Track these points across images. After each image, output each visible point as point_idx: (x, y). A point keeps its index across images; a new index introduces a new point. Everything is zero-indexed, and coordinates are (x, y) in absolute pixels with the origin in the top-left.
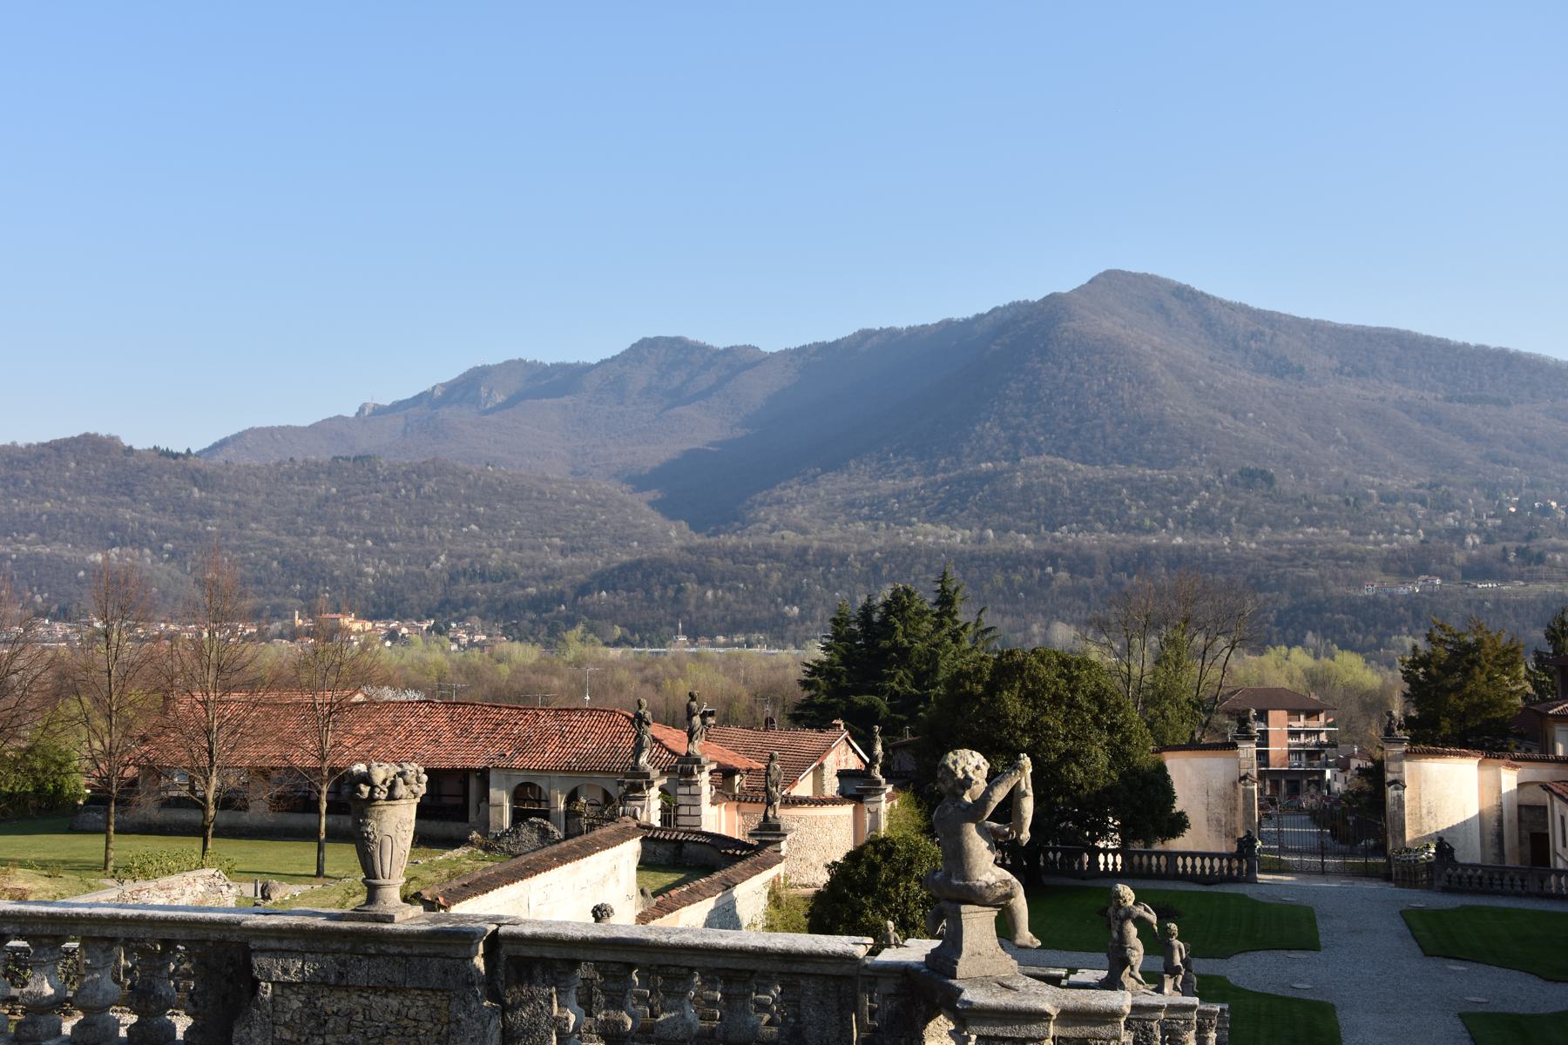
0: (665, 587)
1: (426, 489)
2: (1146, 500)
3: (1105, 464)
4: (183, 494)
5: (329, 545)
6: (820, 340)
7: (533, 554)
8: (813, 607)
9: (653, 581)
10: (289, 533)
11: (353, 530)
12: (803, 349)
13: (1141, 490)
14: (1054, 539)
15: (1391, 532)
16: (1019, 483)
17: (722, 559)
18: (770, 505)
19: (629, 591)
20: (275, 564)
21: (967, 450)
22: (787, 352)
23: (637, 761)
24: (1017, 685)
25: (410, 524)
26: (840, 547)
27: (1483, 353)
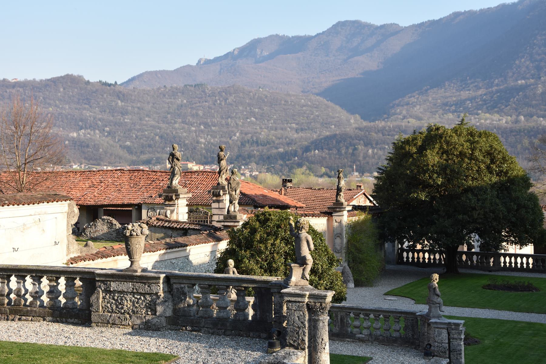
0: (347, 148)
1: (230, 100)
4: (113, 104)
5: (183, 128)
7: (282, 132)
9: (341, 145)
10: (164, 122)
11: (194, 121)
12: (422, 24)
17: (376, 133)
18: (402, 106)
19: (329, 149)
20: (157, 137)
21: (510, 74)
22: (414, 26)
23: (171, 182)
24: (437, 146)
25: (222, 118)
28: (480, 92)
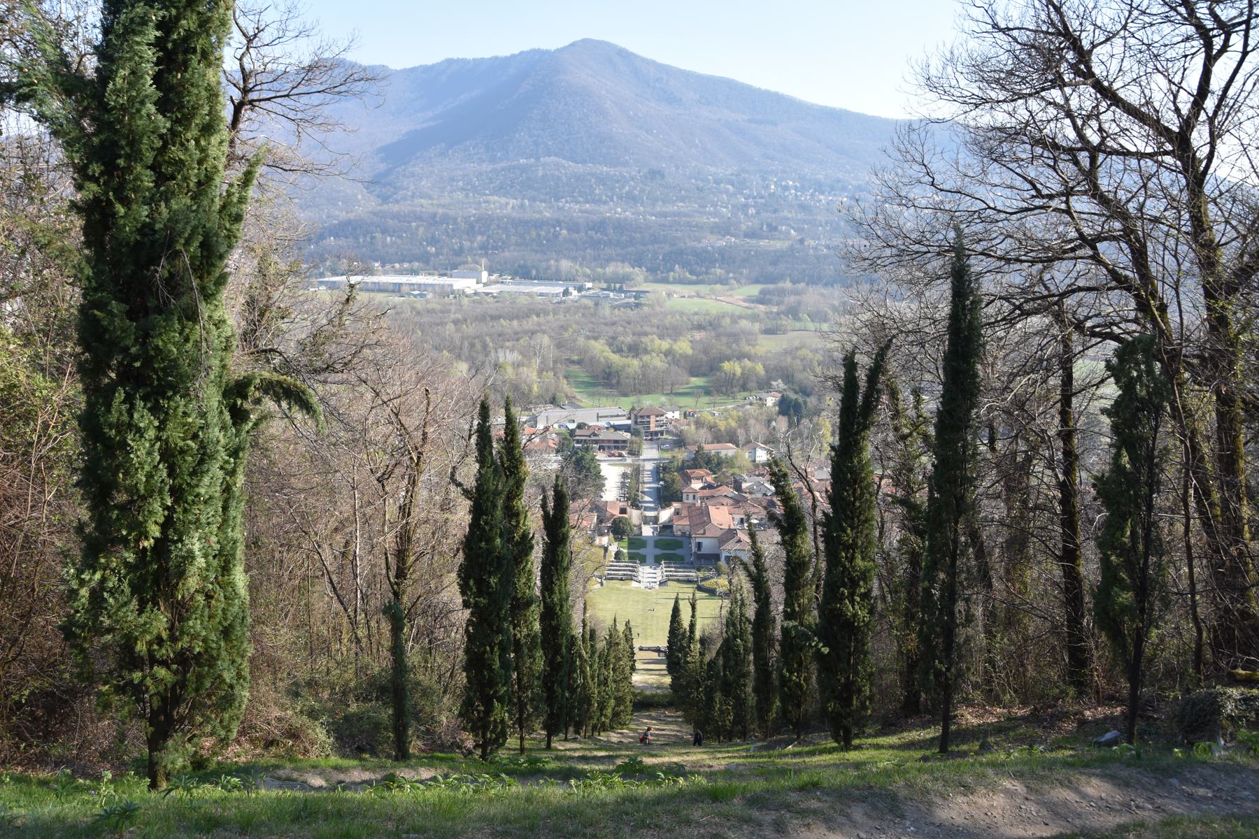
0: (365, 236)
2: (603, 185)
3: (584, 162)
6: (423, 64)
9: (358, 232)
12: (413, 70)
13: (601, 180)
14: (559, 209)
15: (717, 205)
16: (540, 173)
18: (408, 177)
19: (346, 237)
22: (405, 71)
26: (452, 213)
28: (486, 167)
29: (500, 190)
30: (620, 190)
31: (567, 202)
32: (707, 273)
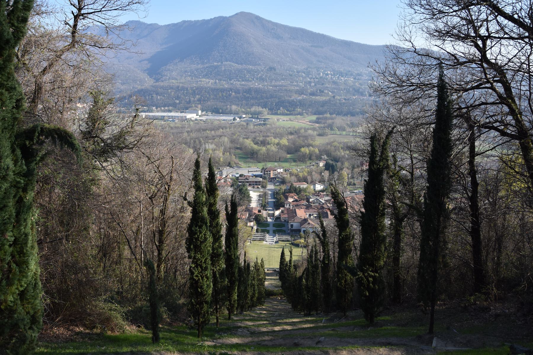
0: (149, 96)
3: (242, 64)
6: (173, 23)
8: (182, 100)
9: (146, 94)
12: (169, 25)
13: (249, 71)
14: (231, 84)
16: (223, 69)
22: (165, 26)
26: (186, 86)
27: (319, 34)
28: (200, 66)
29: (206, 76)
30: (257, 76)
31: (234, 81)
32: (294, 110)
